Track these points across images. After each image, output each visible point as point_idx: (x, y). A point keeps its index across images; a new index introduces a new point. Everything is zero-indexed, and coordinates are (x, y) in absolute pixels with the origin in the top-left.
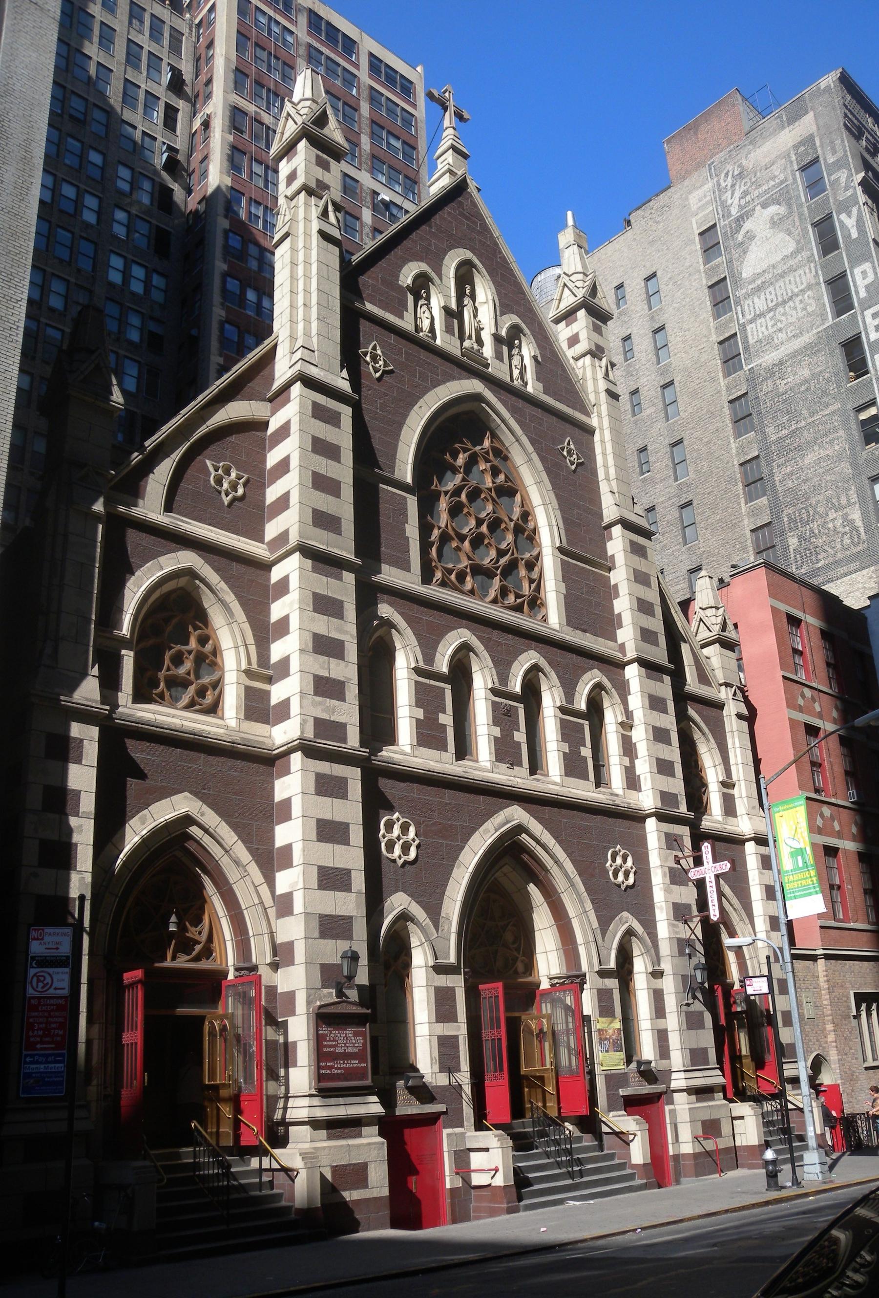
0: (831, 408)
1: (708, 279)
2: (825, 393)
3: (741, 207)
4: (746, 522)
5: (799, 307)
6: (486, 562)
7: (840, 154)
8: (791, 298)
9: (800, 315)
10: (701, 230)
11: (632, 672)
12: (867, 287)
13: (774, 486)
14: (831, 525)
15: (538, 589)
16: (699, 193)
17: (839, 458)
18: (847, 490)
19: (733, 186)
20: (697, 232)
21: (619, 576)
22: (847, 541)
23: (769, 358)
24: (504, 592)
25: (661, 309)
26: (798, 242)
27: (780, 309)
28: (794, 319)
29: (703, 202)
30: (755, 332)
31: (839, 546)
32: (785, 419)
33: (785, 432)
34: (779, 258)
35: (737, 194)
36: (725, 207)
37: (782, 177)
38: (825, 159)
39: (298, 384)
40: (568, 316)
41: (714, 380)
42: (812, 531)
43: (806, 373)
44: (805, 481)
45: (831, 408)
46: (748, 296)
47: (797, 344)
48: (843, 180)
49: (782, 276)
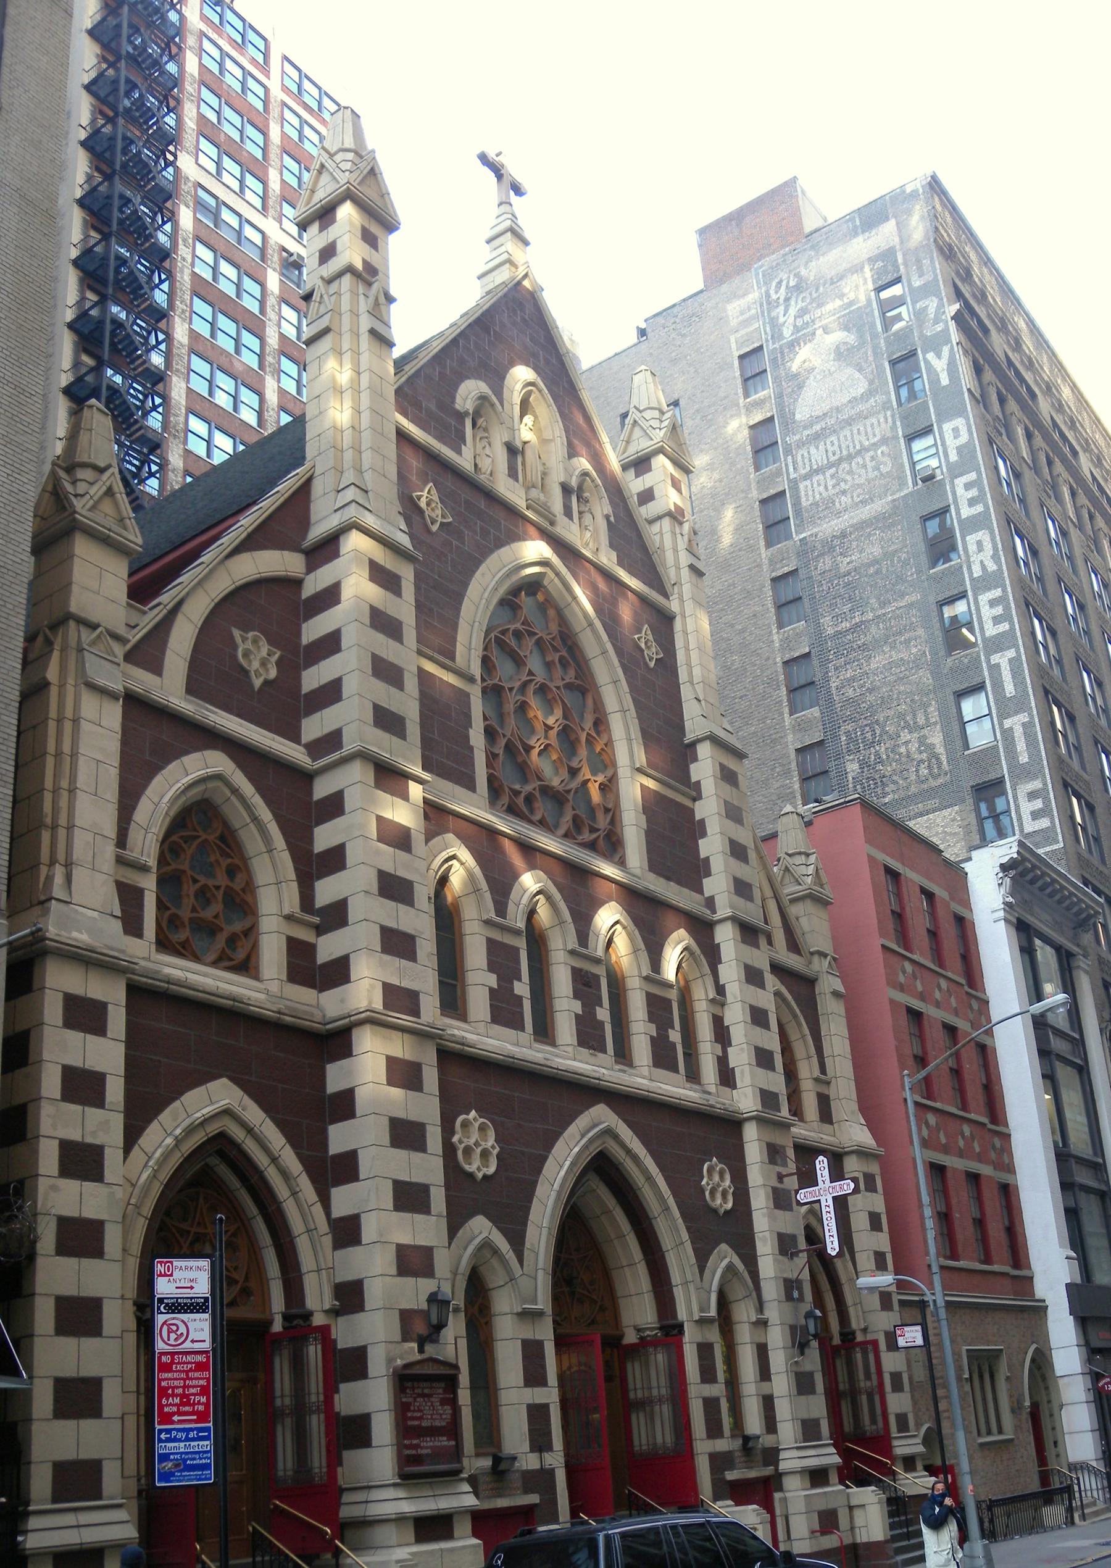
0: (908, 599)
2: (900, 579)
3: (797, 329)
4: (790, 738)
7: (929, 277)
8: (859, 453)
9: (871, 475)
10: (742, 352)
12: (959, 449)
14: (903, 750)
15: (613, 822)
16: (742, 303)
18: (925, 706)
19: (787, 300)
20: (737, 354)
23: (828, 527)
26: (871, 382)
27: (845, 465)
28: (862, 481)
30: (811, 492)
31: (913, 777)
32: (846, 609)
33: (846, 625)
34: (845, 401)
35: (792, 311)
41: (752, 549)
42: (877, 754)
43: (876, 551)
44: (871, 691)
45: (908, 599)
46: (801, 444)
47: (866, 512)
48: (932, 310)
49: (849, 422)
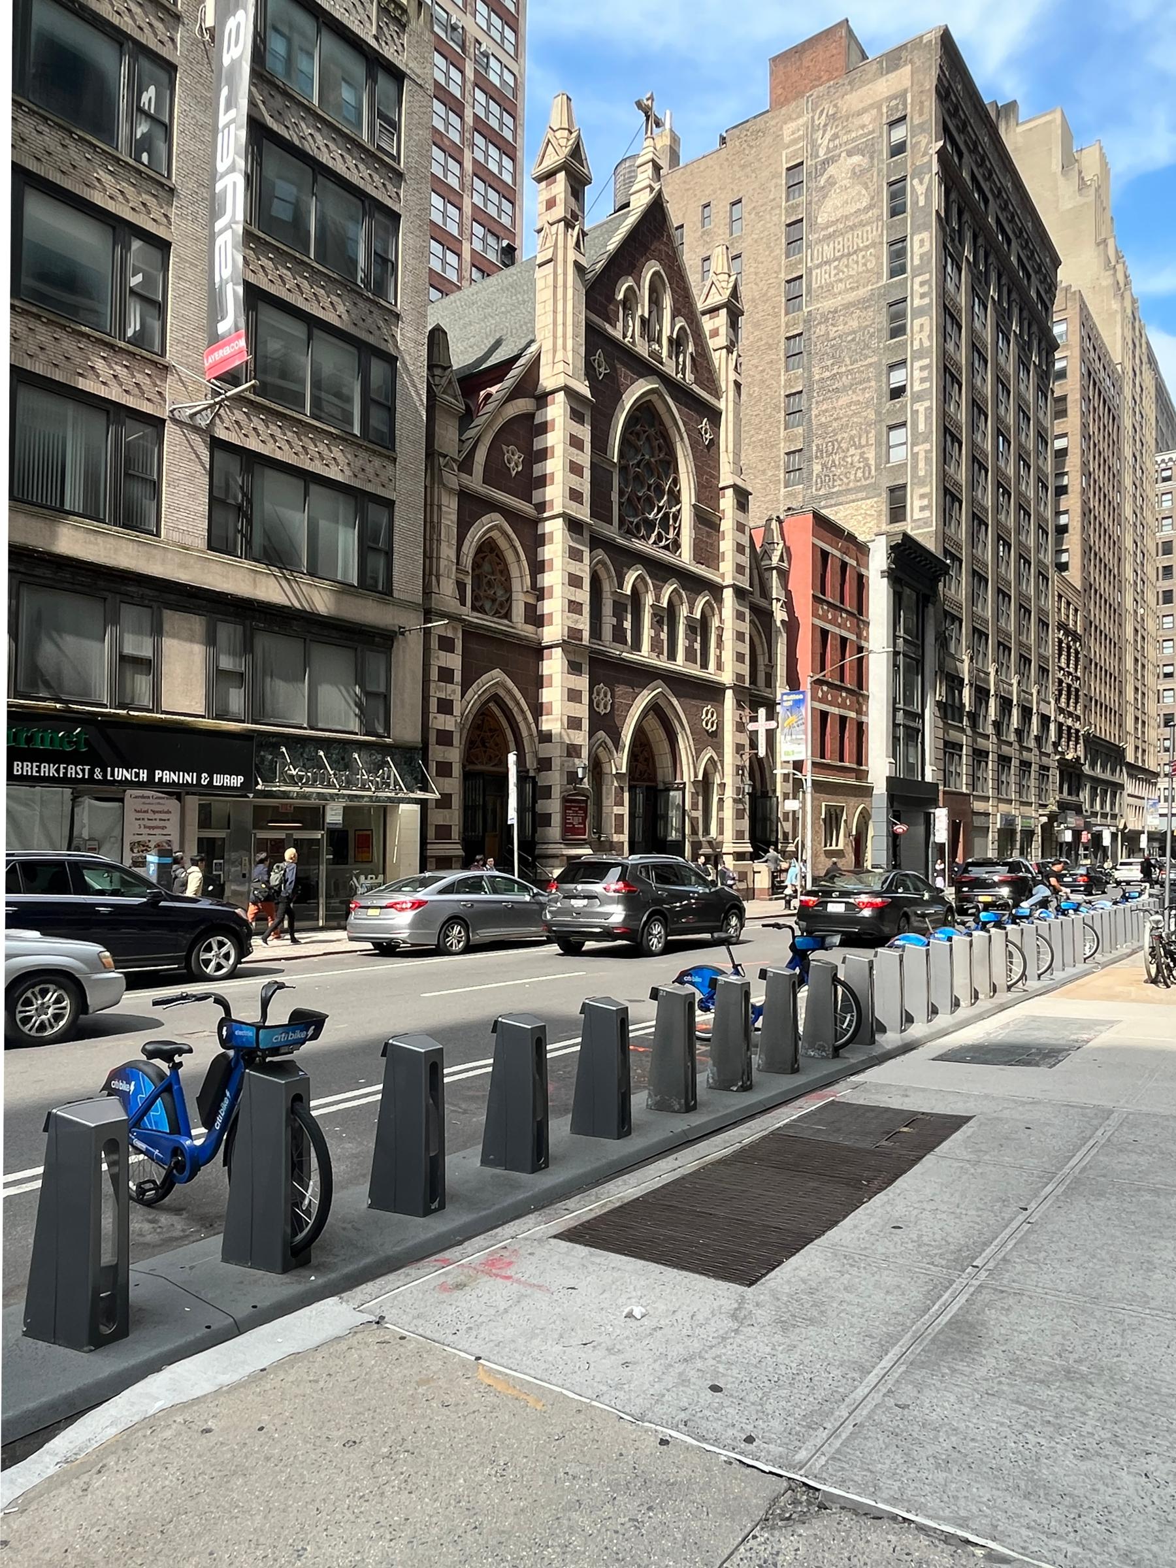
0: (869, 360)
1: (788, 215)
2: (867, 346)
3: (828, 150)
4: (782, 445)
5: (861, 261)
6: (651, 516)
7: (925, 117)
8: (855, 252)
9: (860, 270)
10: (789, 165)
11: (728, 594)
12: (922, 257)
13: (810, 419)
14: (849, 460)
16: (792, 126)
17: (868, 404)
18: (868, 433)
19: (826, 125)
20: (785, 166)
21: (727, 525)
22: (860, 474)
23: (827, 305)
24: (660, 537)
25: (740, 237)
26: (872, 198)
27: (845, 260)
28: (854, 273)
29: (796, 136)
30: (820, 278)
31: (852, 477)
32: (829, 363)
33: (827, 374)
34: (852, 211)
35: (828, 136)
36: (814, 145)
37: (871, 127)
38: (912, 119)
39: (562, 393)
40: (713, 310)
41: (777, 315)
42: (833, 461)
43: (855, 324)
44: (836, 419)
45: (869, 360)
46: (819, 241)
47: (851, 297)
48: (923, 144)
49: (852, 228)
